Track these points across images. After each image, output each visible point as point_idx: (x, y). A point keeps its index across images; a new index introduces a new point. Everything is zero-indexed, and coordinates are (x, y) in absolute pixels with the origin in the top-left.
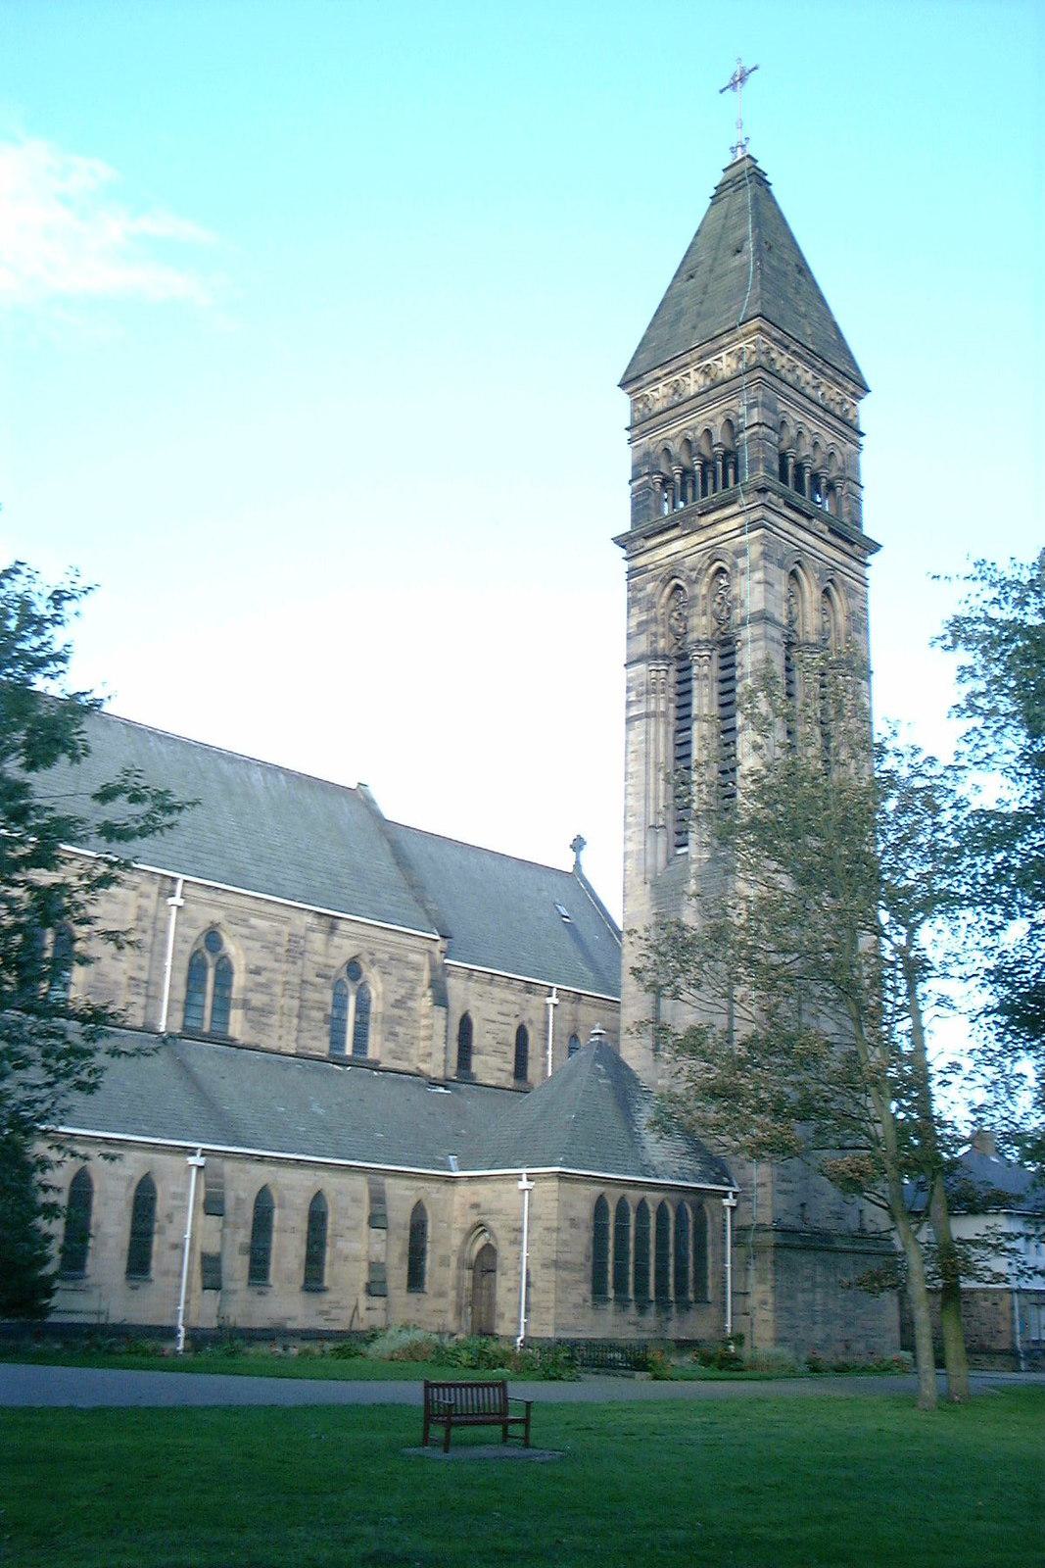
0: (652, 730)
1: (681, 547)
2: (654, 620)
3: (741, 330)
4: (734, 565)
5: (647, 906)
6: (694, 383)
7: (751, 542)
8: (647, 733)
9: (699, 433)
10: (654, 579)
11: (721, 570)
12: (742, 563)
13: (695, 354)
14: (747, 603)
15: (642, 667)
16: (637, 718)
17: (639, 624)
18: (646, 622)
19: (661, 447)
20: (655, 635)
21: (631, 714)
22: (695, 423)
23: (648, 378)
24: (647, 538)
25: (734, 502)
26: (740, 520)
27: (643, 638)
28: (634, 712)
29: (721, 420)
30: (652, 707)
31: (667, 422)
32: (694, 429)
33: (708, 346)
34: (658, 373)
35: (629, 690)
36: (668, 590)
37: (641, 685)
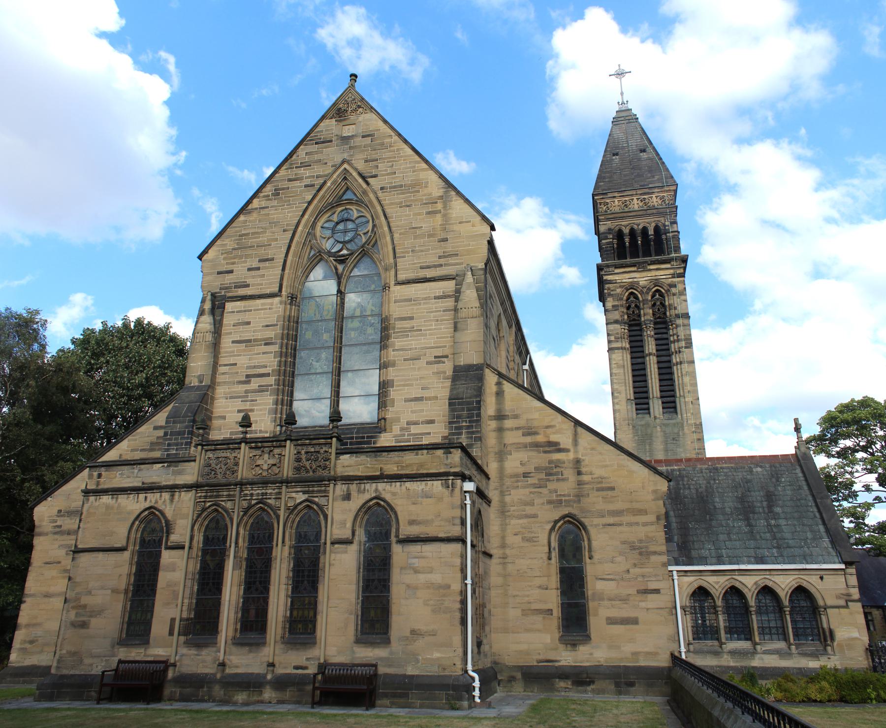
0: (625, 355)
1: (642, 278)
2: (622, 306)
3: (666, 188)
4: (668, 291)
5: (631, 436)
6: (636, 204)
7: (679, 282)
8: (623, 356)
9: (641, 227)
10: (621, 287)
11: (657, 291)
12: (673, 290)
13: (639, 192)
14: (679, 308)
15: (617, 326)
16: (618, 348)
17: (613, 306)
18: (618, 306)
19: (617, 229)
20: (623, 312)
21: (613, 346)
22: (640, 223)
23: (610, 195)
24: (616, 268)
25: (669, 263)
26: (672, 271)
27: (617, 312)
28: (614, 345)
29: (653, 225)
30: (624, 345)
31: (622, 218)
32: (638, 225)
33: (647, 191)
34: (616, 194)
35: (608, 335)
36: (627, 294)
37: (618, 334)
